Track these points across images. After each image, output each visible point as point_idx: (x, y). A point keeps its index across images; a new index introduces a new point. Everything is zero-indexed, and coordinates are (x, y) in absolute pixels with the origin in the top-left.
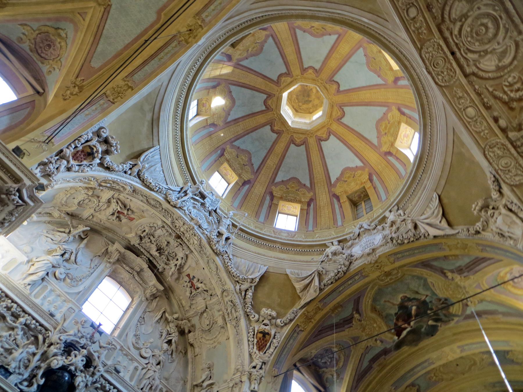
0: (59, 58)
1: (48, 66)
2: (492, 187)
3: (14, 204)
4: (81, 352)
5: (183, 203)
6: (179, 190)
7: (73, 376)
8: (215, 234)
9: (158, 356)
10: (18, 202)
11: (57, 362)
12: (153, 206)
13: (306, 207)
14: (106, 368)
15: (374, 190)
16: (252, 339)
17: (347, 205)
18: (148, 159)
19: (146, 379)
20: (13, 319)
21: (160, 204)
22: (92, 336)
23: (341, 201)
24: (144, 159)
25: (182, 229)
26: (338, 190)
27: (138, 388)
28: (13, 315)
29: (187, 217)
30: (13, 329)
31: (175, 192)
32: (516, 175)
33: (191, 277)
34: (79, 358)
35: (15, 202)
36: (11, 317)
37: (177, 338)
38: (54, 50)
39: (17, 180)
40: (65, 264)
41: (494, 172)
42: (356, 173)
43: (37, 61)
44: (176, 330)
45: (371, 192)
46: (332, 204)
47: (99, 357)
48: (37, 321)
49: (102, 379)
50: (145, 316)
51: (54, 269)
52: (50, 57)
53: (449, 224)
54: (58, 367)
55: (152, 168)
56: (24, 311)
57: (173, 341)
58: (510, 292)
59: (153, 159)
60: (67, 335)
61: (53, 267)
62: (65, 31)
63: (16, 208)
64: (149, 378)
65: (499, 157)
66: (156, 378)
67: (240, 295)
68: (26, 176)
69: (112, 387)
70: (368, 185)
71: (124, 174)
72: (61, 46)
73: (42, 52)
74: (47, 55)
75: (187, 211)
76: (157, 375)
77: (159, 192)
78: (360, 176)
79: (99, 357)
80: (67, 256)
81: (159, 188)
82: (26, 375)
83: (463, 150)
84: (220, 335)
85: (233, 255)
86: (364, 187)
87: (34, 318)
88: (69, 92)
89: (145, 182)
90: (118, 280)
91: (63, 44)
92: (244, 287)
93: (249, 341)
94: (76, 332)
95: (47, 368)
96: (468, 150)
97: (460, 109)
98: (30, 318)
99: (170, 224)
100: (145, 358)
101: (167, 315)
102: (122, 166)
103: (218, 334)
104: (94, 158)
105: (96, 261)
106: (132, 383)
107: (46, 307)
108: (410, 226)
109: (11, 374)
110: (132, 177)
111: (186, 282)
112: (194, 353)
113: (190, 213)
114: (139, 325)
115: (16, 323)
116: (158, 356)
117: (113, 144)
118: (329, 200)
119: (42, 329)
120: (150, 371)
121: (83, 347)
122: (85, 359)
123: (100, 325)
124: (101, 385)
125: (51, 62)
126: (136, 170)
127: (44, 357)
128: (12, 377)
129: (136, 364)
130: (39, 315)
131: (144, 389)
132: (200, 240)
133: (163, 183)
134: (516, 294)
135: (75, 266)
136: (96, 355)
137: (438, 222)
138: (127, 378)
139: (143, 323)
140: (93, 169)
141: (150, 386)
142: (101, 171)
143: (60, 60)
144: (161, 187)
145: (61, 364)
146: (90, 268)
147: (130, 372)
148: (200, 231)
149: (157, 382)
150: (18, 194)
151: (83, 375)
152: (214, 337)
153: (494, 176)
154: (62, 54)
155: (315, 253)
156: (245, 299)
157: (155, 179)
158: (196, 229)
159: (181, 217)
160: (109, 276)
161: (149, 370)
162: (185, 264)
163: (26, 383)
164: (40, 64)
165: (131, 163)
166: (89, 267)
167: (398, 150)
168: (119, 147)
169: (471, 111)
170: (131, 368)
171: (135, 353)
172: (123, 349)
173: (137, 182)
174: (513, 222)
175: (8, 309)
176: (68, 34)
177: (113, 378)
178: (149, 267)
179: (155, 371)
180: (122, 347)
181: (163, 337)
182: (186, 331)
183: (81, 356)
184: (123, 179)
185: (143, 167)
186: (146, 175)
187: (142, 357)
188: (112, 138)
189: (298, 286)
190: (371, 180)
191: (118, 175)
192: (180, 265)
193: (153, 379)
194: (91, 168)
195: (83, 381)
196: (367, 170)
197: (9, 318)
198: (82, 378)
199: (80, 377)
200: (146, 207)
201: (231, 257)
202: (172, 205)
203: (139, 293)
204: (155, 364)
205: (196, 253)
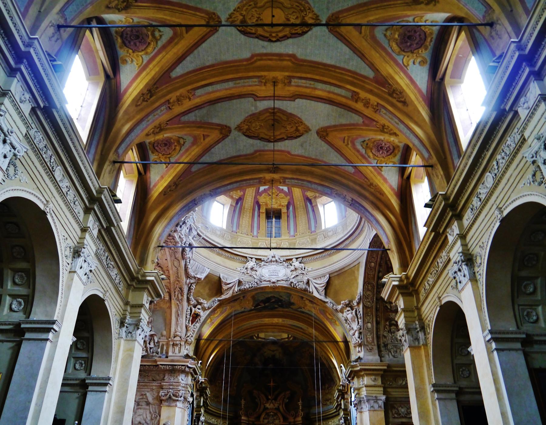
0: (169, 156)
1: (157, 157)
2: (356, 299)
13: (234, 204)
15: (286, 218)
17: (263, 216)
23: (261, 211)
26: (262, 199)
32: (369, 302)
38: (168, 148)
41: (362, 294)
42: (280, 194)
43: (149, 150)
45: (284, 217)
46: (254, 210)
52: (162, 152)
53: (326, 295)
58: (326, 316)
62: (185, 141)
65: (368, 290)
70: (284, 210)
72: (175, 149)
73: (157, 146)
74: (160, 149)
78: (282, 198)
83: (356, 272)
86: (281, 210)
88: (169, 189)
91: (178, 148)
92: (192, 281)
93: (186, 317)
96: (358, 274)
97: (369, 261)
108: (305, 279)
118: (252, 204)
125: (160, 155)
134: (328, 318)
137: (321, 291)
143: (169, 158)
153: (361, 296)
154: (173, 155)
155: (238, 261)
164: (150, 152)
167: (317, 205)
169: (373, 264)
174: (354, 321)
176: (186, 144)
189: (225, 287)
190: (288, 207)
196: (288, 197)
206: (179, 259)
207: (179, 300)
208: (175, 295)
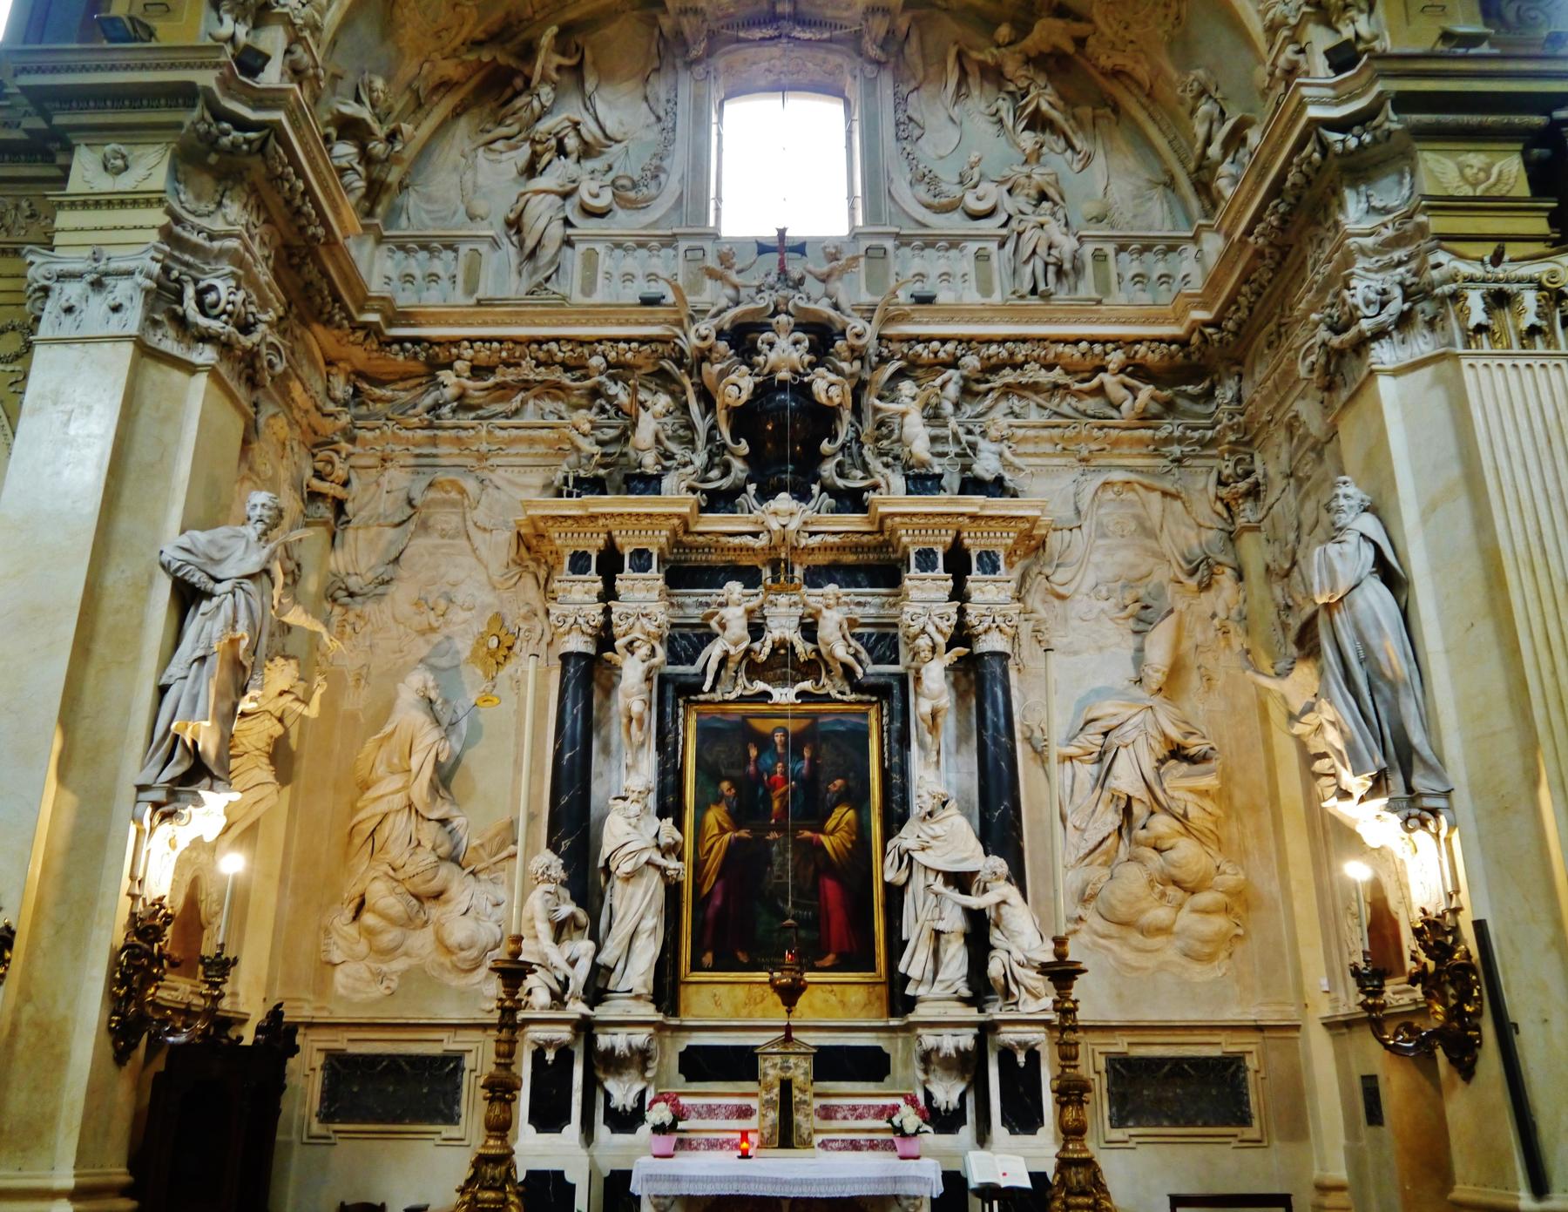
3: (249, 153)
7: (804, 390)
9: (1023, 180)
10: (249, 142)
11: (739, 387)
14: (877, 316)
19: (1027, 262)
20: (578, 374)
22: (783, 271)
27: (1022, 297)
28: (567, 368)
34: (783, 342)
35: (245, 147)
37: (1049, 90)
39: (185, 95)
40: (588, 165)
44: (1031, 73)
47: (836, 307)
48: (628, 340)
50: (910, 112)
51: (575, 200)
54: (745, 397)
56: (582, 342)
57: (1045, 107)
60: (715, 316)
61: (566, 196)
63: (264, 155)
64: (1034, 252)
68: (188, 66)
69: (935, 345)
76: (1055, 231)
79: (836, 307)
80: (571, 143)
82: (700, 459)
87: (616, 340)
94: (730, 292)
95: (729, 415)
98: (606, 346)
100: (990, 214)
101: (975, 55)
105: (660, 88)
106: (996, 298)
109: (658, 478)
112: (1140, 85)
116: (1023, 180)
119: (653, 346)
120: (1026, 236)
121: (776, 313)
122: (799, 335)
123: (782, 233)
124: (904, 357)
127: (707, 399)
128: (667, 483)
129: (973, 247)
130: (620, 324)
131: (1042, 287)
135: (616, 148)
136: (824, 307)
138: (972, 297)
139: (917, 132)
141: (1051, 269)
145: (748, 383)
146: (659, 119)
147: (972, 277)
150: (226, 126)
151: (820, 370)
161: (1020, 234)
163: (714, 473)
166: (653, 119)
171: (954, 223)
172: (905, 240)
177: (919, 323)
179: (1042, 226)
180: (897, 236)
181: (1009, 122)
182: (1070, 48)
183: (783, 336)
187: (975, 216)
193: (1050, 247)
195: (832, 384)
197: (566, 379)
203: (847, 65)
204: (1028, 209)
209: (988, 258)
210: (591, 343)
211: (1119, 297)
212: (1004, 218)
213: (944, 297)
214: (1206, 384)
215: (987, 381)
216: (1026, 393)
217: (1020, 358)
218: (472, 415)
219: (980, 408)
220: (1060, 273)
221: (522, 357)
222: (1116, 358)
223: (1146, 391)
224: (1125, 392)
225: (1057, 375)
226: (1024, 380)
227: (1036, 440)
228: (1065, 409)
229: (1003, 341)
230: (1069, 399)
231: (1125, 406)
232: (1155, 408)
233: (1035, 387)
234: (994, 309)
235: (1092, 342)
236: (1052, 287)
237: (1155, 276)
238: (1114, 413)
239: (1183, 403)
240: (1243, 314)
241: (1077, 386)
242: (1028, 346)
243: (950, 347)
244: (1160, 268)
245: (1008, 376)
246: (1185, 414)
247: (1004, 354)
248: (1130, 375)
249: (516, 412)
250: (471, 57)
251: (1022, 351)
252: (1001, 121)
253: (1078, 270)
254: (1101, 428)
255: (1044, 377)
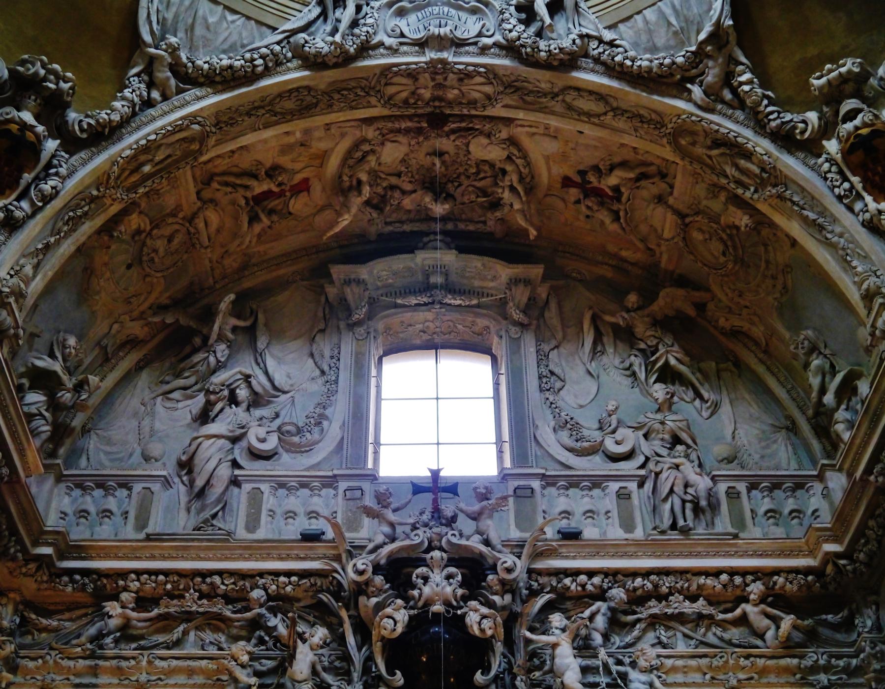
4: (429, 561)
5: (356, 31)
6: (317, 11)
8: (513, 21)
9: (657, 426)
12: (305, 110)
14: (525, 551)
16: (846, 185)
18: (162, 22)
19: (665, 500)
20: (239, 606)
21: (309, 88)
22: (437, 511)
24: (152, 32)
25: (427, 94)
27: (663, 532)
28: (228, 599)
29: (405, 53)
30: (256, 624)
31: (312, 29)
33: (578, 179)
34: (437, 577)
36: (230, 607)
37: (676, 348)
40: (257, 413)
44: (659, 333)
47: (487, 543)
48: (288, 574)
49: (543, 580)
50: (552, 367)
51: (244, 443)
54: (400, 629)
55: (199, 31)
57: (673, 362)
59: (173, 9)
60: (372, 552)
61: (235, 440)
64: (672, 491)
66: (693, 477)
67: (719, 107)
69: (583, 578)
71: (152, 111)
75: (388, 41)
76: (689, 471)
77: (274, 64)
79: (487, 543)
80: (242, 393)
81: (262, 57)
84: (770, 248)
85: (611, 27)
87: (276, 574)
89: (218, 79)
90: (418, 342)
93: (840, 198)
94: (387, 529)
98: (266, 580)
99: (386, 112)
100: (629, 456)
101: (608, 318)
102: (124, 98)
103: (766, 251)
104: (36, 149)
105: (325, 347)
106: (639, 533)
107: (292, 530)
110: (176, 100)
111: (578, 202)
112: (757, 343)
113: (402, 35)
114: (551, 399)
115: (250, 610)
116: (657, 426)
117: (36, 74)
120: (663, 476)
121: (430, 549)
122: (452, 570)
123: (435, 474)
124: (553, 590)
126: (164, 74)
127: (363, 630)
129: (614, 486)
130: (281, 559)
131: (681, 523)
132: (491, 73)
133: (262, 37)
135: (283, 398)
136: (475, 543)
138: (616, 533)
139: (558, 384)
140: (63, 171)
141: (688, 506)
142: (91, 159)
144: (264, 51)
145: (402, 616)
146: (323, 373)
147: (615, 514)
148: (468, 53)
149: (702, 483)
151: (473, 603)
152: (763, 265)
156: (742, 105)
157: (232, 48)
158: (450, 59)
159: (389, 67)
160: (387, 353)
161: (657, 474)
162: (528, 164)
165: (135, 70)
166: (318, 372)
168: (56, 66)
170: (606, 500)
171: (595, 465)
172: (550, 480)
173: (199, 99)
175: (210, 595)
177: (567, 557)
178: (461, 250)
180: (544, 475)
181: (642, 376)
182: (691, 312)
183: (436, 571)
184: (159, 123)
185: (173, 51)
186: (199, 63)
187: (615, 458)
188: (23, 63)
191: (138, 128)
192: (521, 179)
194: (57, 174)
195: (484, 617)
198: (476, 611)
199: (471, 613)
200: (297, 127)
201: (608, 36)
202: (336, 66)
203: (492, 325)
204: (664, 452)
205: (521, 115)
206: (560, 84)
207: (762, 184)
208: (739, 183)
209: (628, 496)
210: (252, 576)
211: (754, 532)
212: (642, 459)
213: (590, 532)
214: (846, 612)
215: (635, 613)
216: (672, 624)
217: (664, 590)
218: (134, 645)
219: (628, 639)
220: (697, 510)
221: (186, 589)
222: (756, 589)
223: (788, 622)
224: (767, 622)
225: (700, 605)
226: (669, 611)
227: (685, 670)
228: (711, 638)
229: (646, 574)
230: (714, 629)
231: (770, 635)
232: (798, 636)
233: (681, 618)
234: (637, 543)
235: (732, 572)
236: (690, 523)
237: (786, 511)
238: (759, 642)
239: (825, 632)
240: (873, 546)
241: (721, 616)
242: (671, 578)
243: (596, 580)
244: (790, 504)
245: (654, 608)
246: (827, 642)
247: (649, 586)
248: (770, 605)
249: (178, 643)
250: (156, 319)
251: (666, 583)
252: (634, 374)
253: (714, 507)
254: (747, 657)
255: (688, 608)
